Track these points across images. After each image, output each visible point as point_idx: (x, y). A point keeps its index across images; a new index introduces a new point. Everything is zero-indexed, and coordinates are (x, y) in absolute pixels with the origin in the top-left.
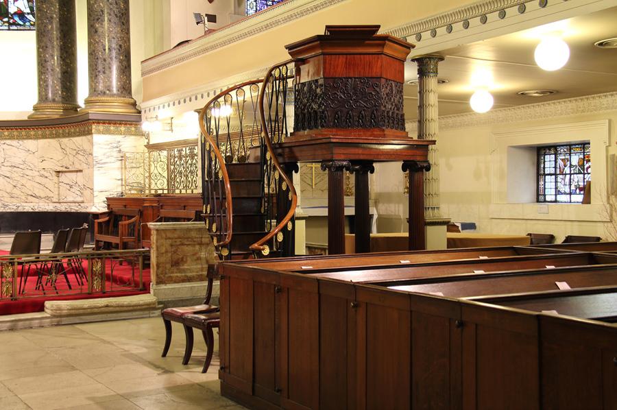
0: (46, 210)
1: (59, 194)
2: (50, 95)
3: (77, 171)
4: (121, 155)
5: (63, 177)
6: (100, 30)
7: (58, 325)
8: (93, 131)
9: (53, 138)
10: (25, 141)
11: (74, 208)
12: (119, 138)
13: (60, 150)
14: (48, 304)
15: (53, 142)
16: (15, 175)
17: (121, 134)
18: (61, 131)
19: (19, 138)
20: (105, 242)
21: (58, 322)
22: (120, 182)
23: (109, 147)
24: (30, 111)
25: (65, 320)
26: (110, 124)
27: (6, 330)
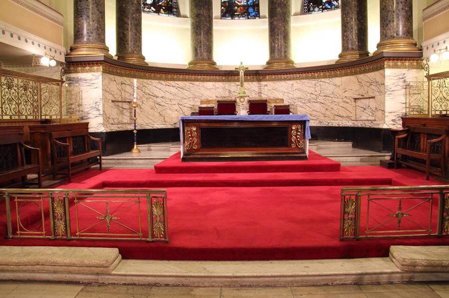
0: (347, 126)
1: (356, 114)
2: (350, 46)
3: (369, 98)
4: (406, 84)
5: (359, 103)
8: (385, 66)
9: (353, 75)
10: (333, 79)
11: (368, 125)
12: (404, 71)
13: (357, 83)
14: (395, 250)
15: (352, 78)
16: (327, 102)
17: (406, 68)
18: (358, 70)
19: (330, 77)
20: (402, 155)
21: (411, 278)
22: (404, 105)
23: (397, 78)
24: (337, 58)
26: (397, 60)
27: (351, 284)
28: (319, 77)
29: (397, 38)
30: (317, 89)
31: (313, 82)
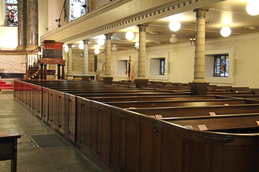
2: (20, 44)
6: (30, 29)
7: (3, 94)
15: (20, 56)
16: (12, 64)
24: (16, 48)
25: (5, 93)
28: (9, 55)
29: (32, 45)
30: (8, 59)
31: (7, 56)
